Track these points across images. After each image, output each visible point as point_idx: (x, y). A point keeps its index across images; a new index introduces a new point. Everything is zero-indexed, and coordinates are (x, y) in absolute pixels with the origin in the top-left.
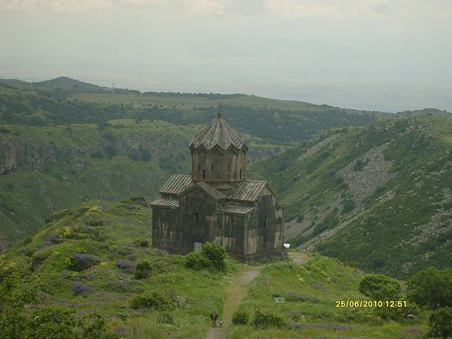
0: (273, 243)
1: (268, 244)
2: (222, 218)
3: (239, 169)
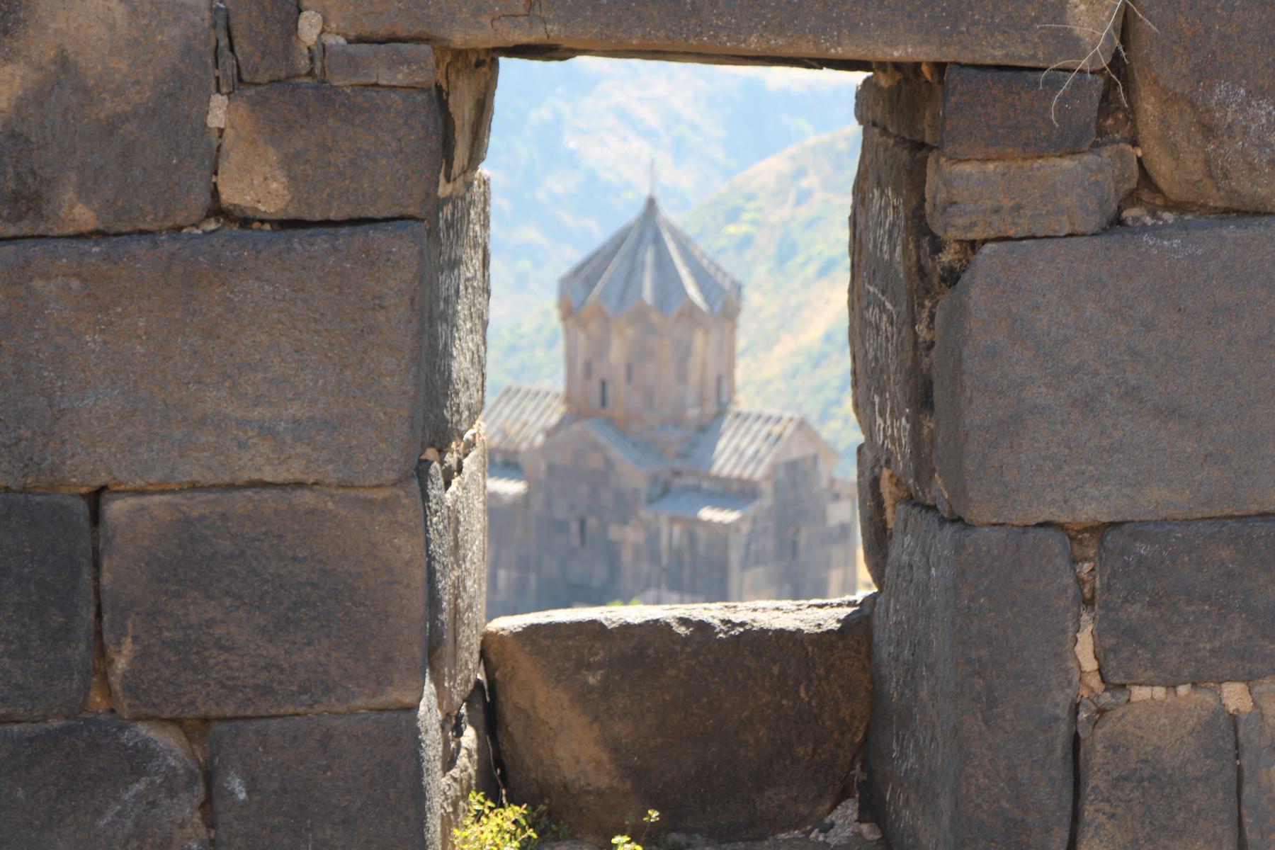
3: (711, 376)
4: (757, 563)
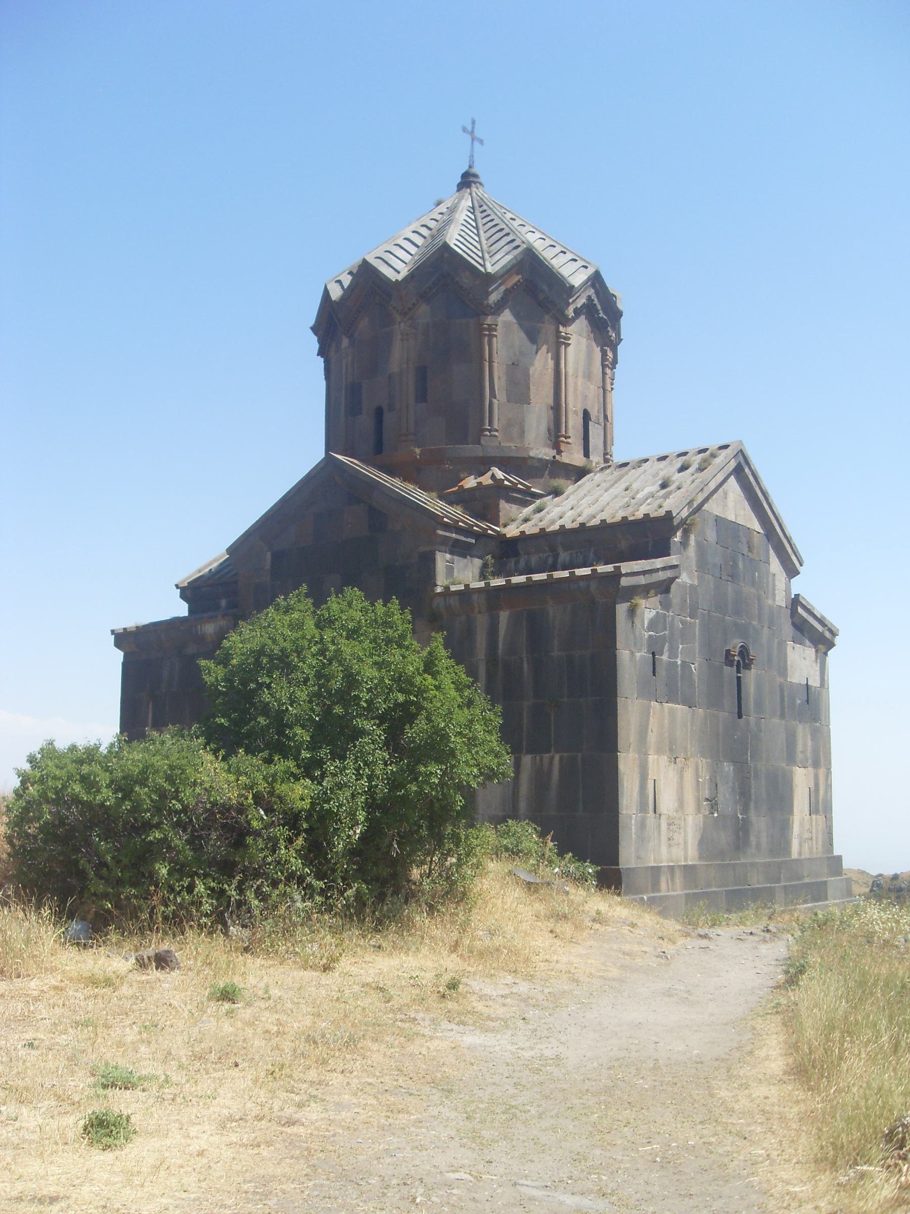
0: (784, 827)
1: (760, 823)
4: (671, 698)
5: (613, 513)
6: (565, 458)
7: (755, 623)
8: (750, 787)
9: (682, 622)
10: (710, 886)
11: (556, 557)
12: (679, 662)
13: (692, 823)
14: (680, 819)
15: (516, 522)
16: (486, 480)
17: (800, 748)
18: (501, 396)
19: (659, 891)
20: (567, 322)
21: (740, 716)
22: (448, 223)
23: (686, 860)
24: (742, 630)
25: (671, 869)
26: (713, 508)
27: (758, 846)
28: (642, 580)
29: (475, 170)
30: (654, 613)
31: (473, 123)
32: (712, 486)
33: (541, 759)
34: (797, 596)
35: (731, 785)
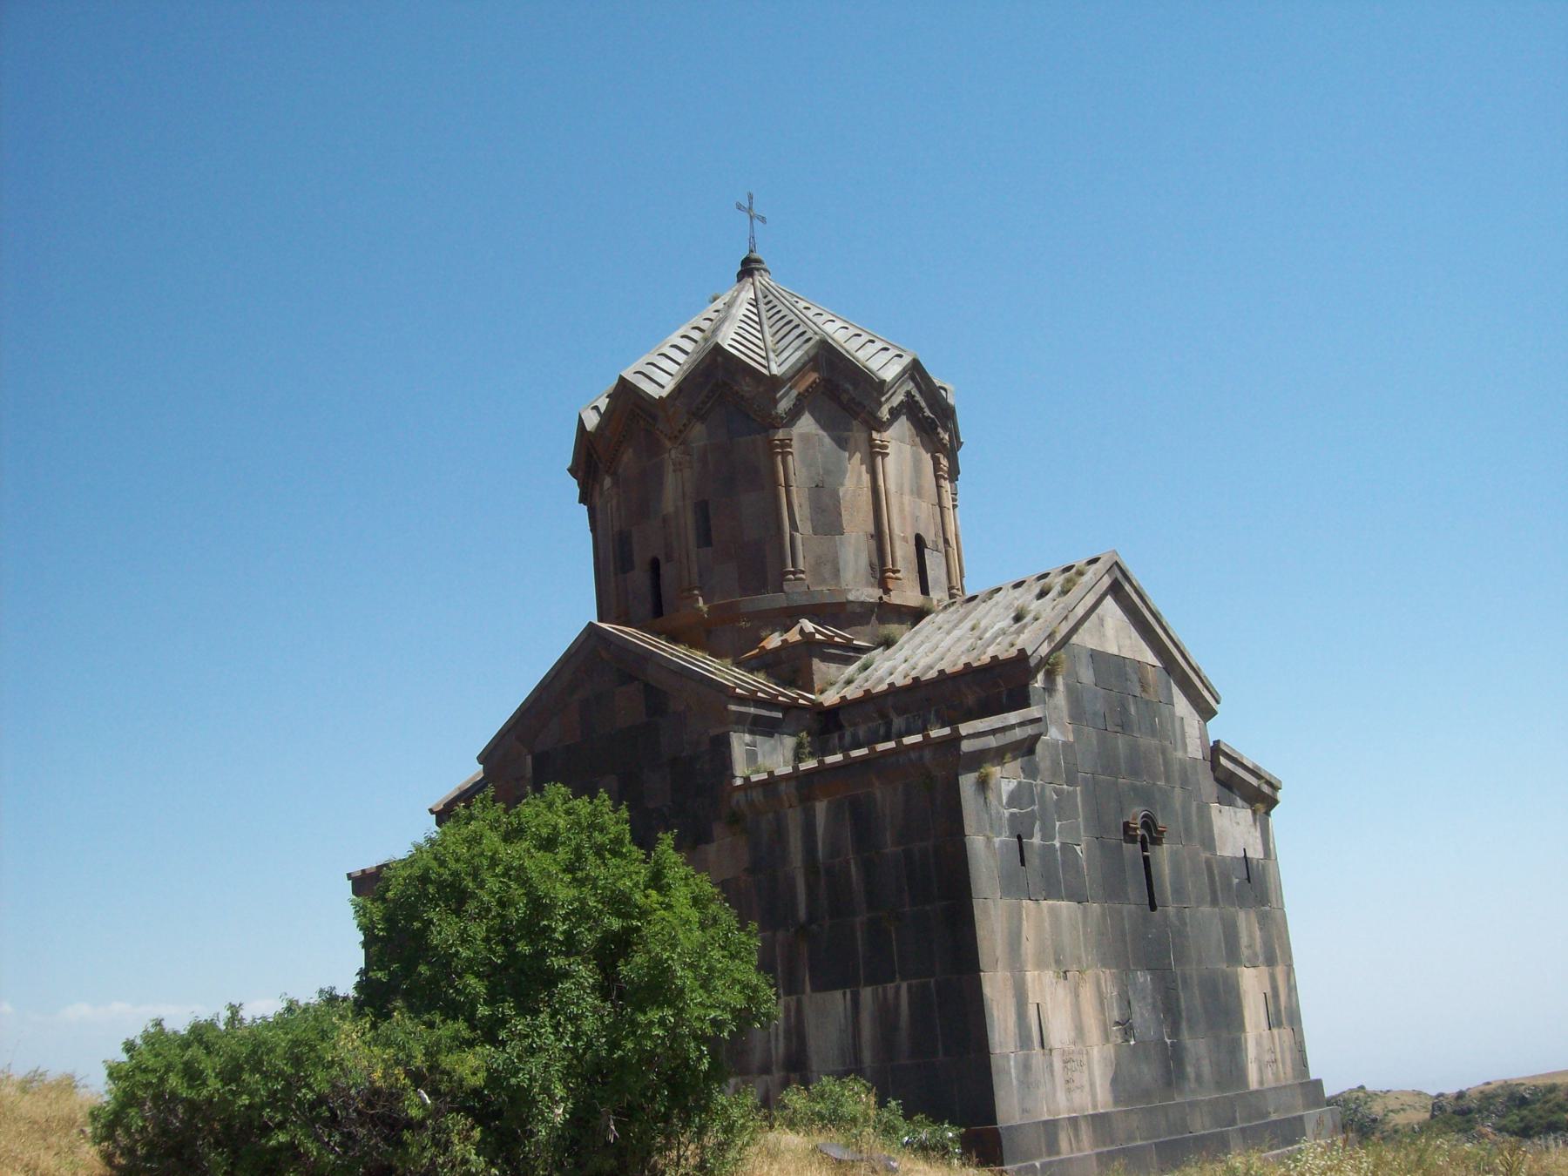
0: (1233, 1050)
1: (1197, 1047)
2: (780, 832)
5: (953, 662)
6: (896, 598)
7: (1161, 783)
8: (1178, 999)
9: (1057, 792)
10: (1131, 1138)
11: (889, 724)
12: (1058, 845)
13: (1098, 1059)
14: (1080, 1053)
15: (836, 685)
16: (793, 636)
17: (1244, 941)
18: (805, 526)
19: (1058, 1153)
20: (882, 426)
21: (1153, 907)
22: (723, 321)
23: (1095, 1106)
24: (1145, 796)
25: (1073, 1121)
26: (1085, 639)
27: (1199, 1077)
28: (992, 742)
29: (755, 255)
30: (1013, 784)
31: (751, 197)
32: (1080, 611)
33: (885, 990)
34: (1217, 743)
35: (1150, 1000)
